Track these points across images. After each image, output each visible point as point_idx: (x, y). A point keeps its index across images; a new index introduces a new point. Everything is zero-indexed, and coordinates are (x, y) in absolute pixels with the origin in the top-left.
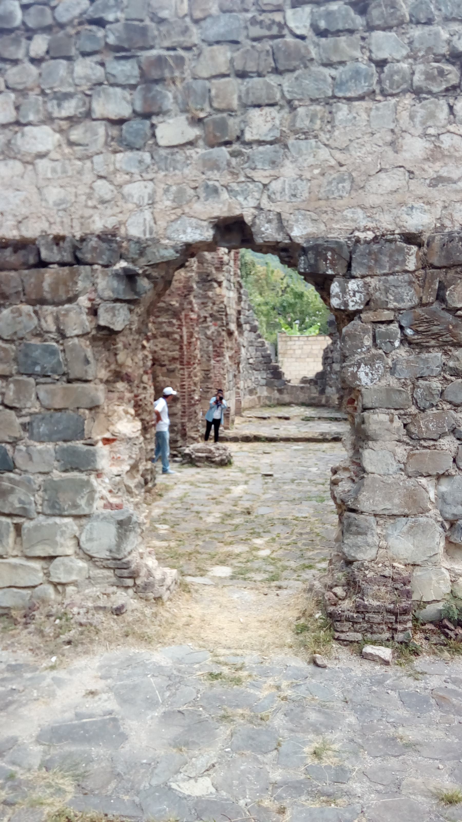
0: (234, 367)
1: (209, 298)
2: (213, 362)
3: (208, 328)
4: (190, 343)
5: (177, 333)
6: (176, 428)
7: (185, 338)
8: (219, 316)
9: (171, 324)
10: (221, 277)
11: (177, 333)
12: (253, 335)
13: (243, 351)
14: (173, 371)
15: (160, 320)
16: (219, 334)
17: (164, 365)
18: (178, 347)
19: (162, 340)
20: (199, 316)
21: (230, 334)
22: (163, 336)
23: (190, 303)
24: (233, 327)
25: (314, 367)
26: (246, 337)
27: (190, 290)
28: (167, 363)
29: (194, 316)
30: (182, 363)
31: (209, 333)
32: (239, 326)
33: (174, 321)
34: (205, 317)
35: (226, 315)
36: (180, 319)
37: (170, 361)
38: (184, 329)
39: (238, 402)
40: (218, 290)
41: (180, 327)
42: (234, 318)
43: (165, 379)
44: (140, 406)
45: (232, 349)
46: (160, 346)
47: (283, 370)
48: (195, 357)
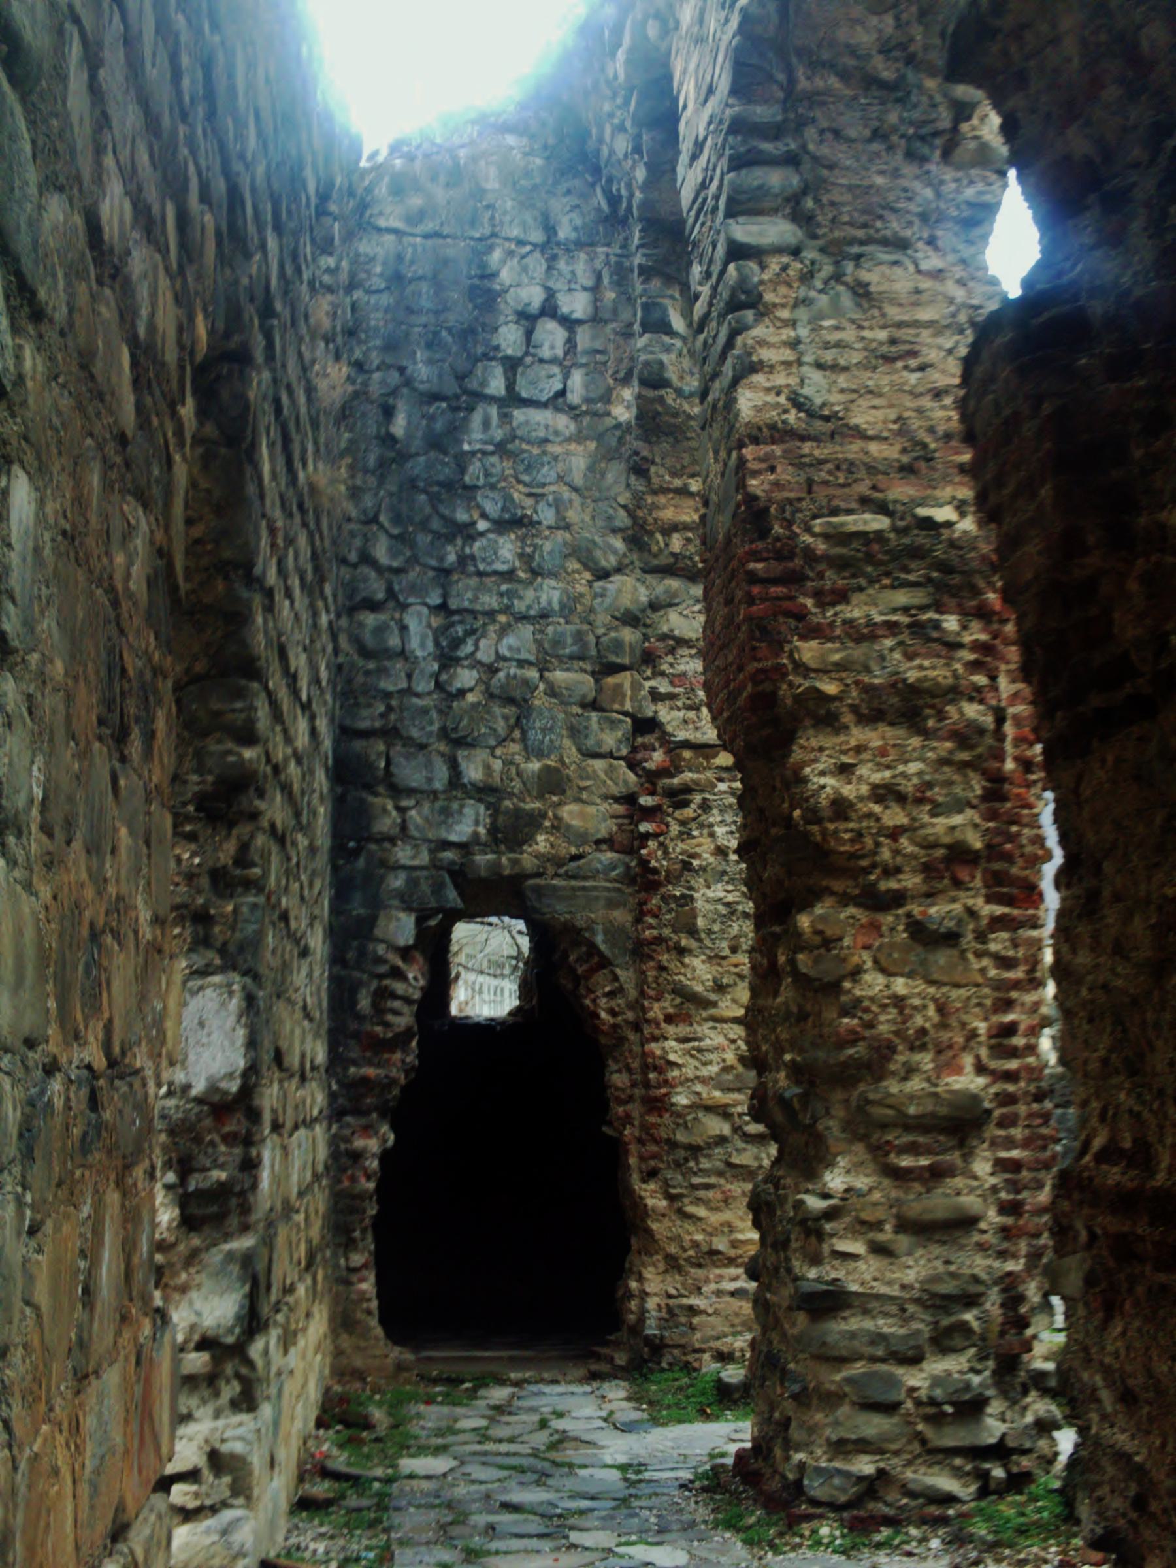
6: (969, 1316)
11: (976, 695)
14: (925, 936)
15: (855, 611)
17: (898, 899)
18: (978, 785)
19: (873, 737)
22: (872, 716)
28: (911, 881)
33: (951, 623)
37: (927, 869)
43: (900, 985)
46: (871, 774)
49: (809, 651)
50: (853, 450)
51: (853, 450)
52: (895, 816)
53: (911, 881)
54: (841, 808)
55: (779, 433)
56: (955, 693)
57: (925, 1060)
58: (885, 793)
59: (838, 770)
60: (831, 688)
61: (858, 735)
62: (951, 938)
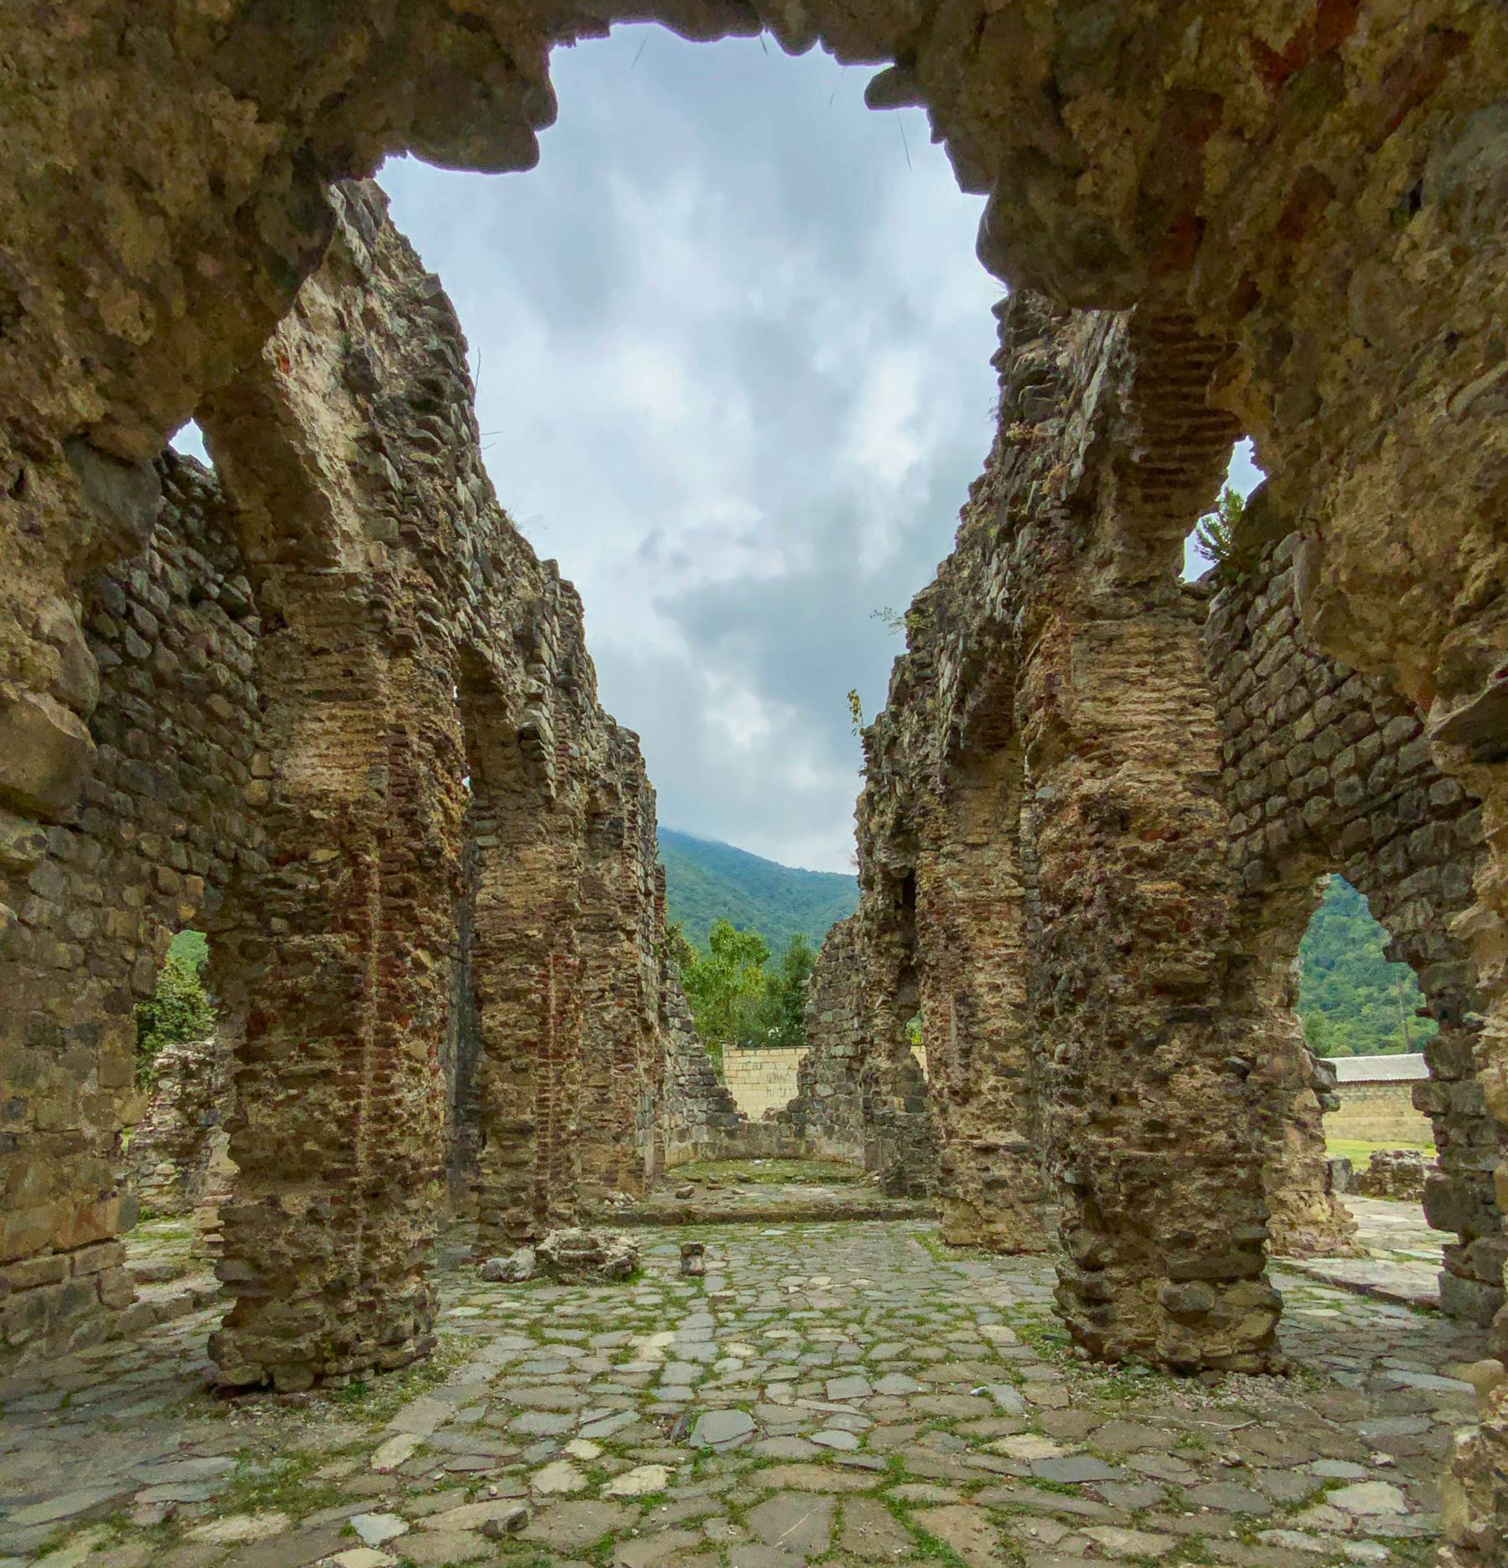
0: (653, 1088)
1: (608, 956)
2: (613, 1071)
3: (606, 1008)
4: (562, 1013)
5: (536, 991)
7: (553, 1003)
8: (629, 989)
9: (524, 973)
10: (632, 925)
11: (536, 991)
12: (685, 1037)
13: (669, 1061)
15: (503, 966)
16: (627, 1021)
18: (537, 1020)
20: (583, 962)
21: (647, 1028)
22: (506, 999)
23: (567, 935)
24: (652, 1016)
25: (784, 1094)
26: (673, 1040)
27: (569, 912)
29: (574, 961)
30: (543, 1053)
31: (608, 1017)
32: (663, 1019)
33: (533, 968)
34: (603, 991)
35: (641, 993)
36: (545, 966)
37: (518, 1048)
38: (552, 983)
39: (660, 1151)
40: (626, 945)
41: (545, 977)
42: (654, 1000)
44: (393, 1119)
45: (649, 1055)
46: (500, 1018)
47: (735, 1097)
48: (573, 1043)
49: (486, 978)
50: (509, 912)
51: (509, 912)
52: (508, 1031)
53: (512, 1052)
54: (490, 1030)
55: (489, 908)
56: (530, 991)
57: (514, 1110)
58: (504, 1024)
59: (493, 1018)
60: (490, 990)
61: (502, 1005)
62: (524, 1070)
